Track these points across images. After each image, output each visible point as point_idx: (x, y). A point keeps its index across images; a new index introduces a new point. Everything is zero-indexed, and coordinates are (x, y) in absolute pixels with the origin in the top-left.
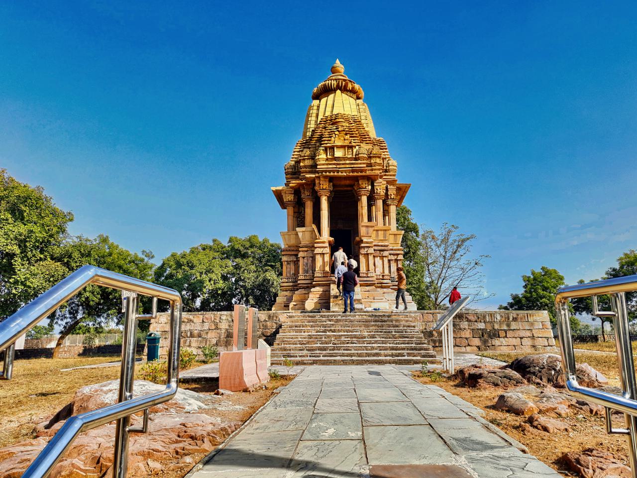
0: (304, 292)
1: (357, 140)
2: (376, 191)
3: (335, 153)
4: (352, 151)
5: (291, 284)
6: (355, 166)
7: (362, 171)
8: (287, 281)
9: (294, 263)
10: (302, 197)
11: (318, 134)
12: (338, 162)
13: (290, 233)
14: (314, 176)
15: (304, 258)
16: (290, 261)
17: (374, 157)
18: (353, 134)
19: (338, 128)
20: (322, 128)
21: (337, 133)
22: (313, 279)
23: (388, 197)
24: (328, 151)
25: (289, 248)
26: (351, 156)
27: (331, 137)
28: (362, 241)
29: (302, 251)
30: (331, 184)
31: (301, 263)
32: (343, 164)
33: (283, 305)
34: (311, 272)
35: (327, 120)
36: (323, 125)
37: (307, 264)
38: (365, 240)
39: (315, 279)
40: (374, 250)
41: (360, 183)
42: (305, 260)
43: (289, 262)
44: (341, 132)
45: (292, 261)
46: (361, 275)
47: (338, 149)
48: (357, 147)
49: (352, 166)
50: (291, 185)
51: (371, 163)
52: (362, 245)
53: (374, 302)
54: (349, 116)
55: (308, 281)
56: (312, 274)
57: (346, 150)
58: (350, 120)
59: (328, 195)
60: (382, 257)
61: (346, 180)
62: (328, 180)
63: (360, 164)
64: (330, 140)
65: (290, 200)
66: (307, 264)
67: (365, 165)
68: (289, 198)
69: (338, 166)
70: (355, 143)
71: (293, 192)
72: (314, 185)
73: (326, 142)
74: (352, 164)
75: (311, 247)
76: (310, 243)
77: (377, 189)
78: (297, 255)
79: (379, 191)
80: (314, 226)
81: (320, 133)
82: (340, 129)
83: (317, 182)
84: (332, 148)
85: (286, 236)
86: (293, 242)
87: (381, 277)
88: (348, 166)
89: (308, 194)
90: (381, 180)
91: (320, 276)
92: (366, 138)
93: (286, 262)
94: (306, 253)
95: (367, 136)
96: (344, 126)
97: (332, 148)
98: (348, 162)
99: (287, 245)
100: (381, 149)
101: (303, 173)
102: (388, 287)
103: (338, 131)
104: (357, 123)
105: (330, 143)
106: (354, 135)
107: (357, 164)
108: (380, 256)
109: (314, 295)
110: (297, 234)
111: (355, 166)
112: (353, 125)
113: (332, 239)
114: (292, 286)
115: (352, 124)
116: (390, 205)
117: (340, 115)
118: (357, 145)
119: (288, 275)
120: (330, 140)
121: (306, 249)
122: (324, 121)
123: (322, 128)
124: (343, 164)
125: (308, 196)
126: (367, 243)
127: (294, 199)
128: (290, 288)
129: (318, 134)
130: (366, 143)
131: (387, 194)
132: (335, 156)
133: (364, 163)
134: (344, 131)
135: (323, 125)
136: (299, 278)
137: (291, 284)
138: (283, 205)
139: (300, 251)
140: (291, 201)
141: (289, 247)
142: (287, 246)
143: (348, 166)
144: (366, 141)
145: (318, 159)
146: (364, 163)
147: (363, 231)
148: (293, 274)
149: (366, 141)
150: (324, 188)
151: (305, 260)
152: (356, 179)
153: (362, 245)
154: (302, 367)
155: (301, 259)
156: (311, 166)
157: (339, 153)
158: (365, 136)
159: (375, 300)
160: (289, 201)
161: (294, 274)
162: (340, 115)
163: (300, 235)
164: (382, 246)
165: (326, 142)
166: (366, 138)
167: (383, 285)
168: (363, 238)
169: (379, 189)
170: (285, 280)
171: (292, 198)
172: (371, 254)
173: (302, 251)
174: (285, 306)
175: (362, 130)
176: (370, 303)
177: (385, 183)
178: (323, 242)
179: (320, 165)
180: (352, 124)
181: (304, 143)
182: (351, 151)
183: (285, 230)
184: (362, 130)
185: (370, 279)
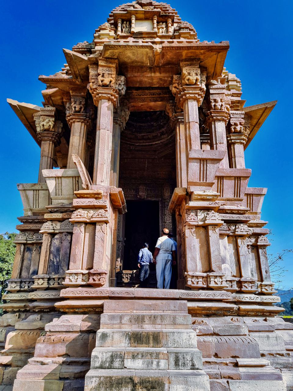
2: (213, 104)
3: (133, 25)
4: (167, 27)
8: (18, 288)
15: (53, 235)
16: (33, 244)
24: (120, 25)
25: (35, 217)
28: (189, 195)
29: (52, 220)
30: (123, 78)
38: (197, 191)
41: (185, 71)
43: (31, 247)
46: (189, 283)
47: (139, 22)
52: (192, 204)
61: (155, 72)
62: (114, 65)
66: (58, 250)
68: (44, 123)
71: (53, 114)
77: (215, 101)
79: (219, 105)
83: (92, 72)
87: (235, 287)
91: (80, 282)
93: (23, 247)
97: (127, 20)
99: (31, 210)
108: (228, 236)
109: (50, 347)
113: (117, 190)
121: (59, 216)
128: (22, 305)
132: (132, 30)
141: (34, 214)
150: (107, 81)
153: (192, 204)
159: (241, 370)
160: (45, 130)
164: (232, 212)
167: (243, 307)
168: (192, 189)
169: (218, 98)
170: (14, 285)
171: (51, 124)
172: (215, 225)
173: (52, 220)
178: (97, 196)
182: (164, 26)
185: (217, 295)
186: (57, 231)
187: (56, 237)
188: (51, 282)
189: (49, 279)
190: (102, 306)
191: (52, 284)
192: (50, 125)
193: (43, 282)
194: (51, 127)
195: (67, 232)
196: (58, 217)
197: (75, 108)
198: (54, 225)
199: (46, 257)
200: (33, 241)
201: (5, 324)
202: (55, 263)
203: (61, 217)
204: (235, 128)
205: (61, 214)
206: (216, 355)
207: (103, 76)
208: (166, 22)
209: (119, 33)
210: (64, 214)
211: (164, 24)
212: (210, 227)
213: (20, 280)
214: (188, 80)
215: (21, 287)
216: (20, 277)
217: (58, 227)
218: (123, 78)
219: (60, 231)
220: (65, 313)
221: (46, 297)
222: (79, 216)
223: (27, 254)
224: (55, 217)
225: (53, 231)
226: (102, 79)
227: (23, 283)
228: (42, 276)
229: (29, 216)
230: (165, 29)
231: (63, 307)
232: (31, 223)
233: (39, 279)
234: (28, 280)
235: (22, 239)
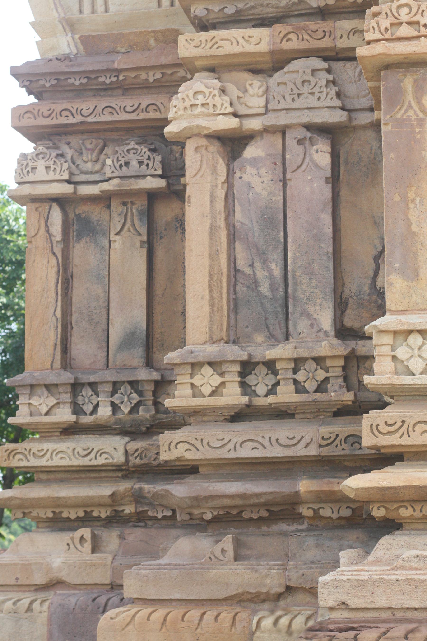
0: (239, 576)
5: (113, 449)
8: (65, 415)
15: (233, 144)
16: (105, 199)
25: (92, 64)
34: (326, 320)
37: (277, 220)
42: (256, 175)
43: (96, 213)
45: (125, 196)
55: (283, 431)
56: (330, 347)
66: (277, 220)
93: (56, 215)
94: (254, 93)
99: (70, 25)
114: (124, 471)
119: (85, 350)
121: (257, 41)
128: (104, 491)
136: (178, 399)
137: (113, 449)
139: (188, 69)
141: (90, 44)
142: (65, 44)
148: (128, 341)
155: (203, 175)
161: (151, 342)
186: (254, 124)
187: (251, 152)
188: (260, 382)
189: (247, 367)
191: (261, 390)
193: (216, 380)
195: (308, 127)
196: (250, 48)
198: (234, 91)
199: (213, 257)
200: (105, 186)
201: (39, 579)
202: (265, 288)
203: (264, 47)
205: (263, 33)
210: (280, 28)
213: (67, 377)
215: (77, 410)
216: (67, 363)
217: (256, 103)
219: (272, 120)
220: (391, 526)
221: (246, 452)
222: (405, 31)
223: (84, 254)
224: (237, 49)
225: (231, 123)
227: (87, 392)
228: (212, 351)
229: (66, 58)
231: (388, 495)
232: (79, 92)
233: (196, 366)
234: (110, 376)
235: (51, 176)
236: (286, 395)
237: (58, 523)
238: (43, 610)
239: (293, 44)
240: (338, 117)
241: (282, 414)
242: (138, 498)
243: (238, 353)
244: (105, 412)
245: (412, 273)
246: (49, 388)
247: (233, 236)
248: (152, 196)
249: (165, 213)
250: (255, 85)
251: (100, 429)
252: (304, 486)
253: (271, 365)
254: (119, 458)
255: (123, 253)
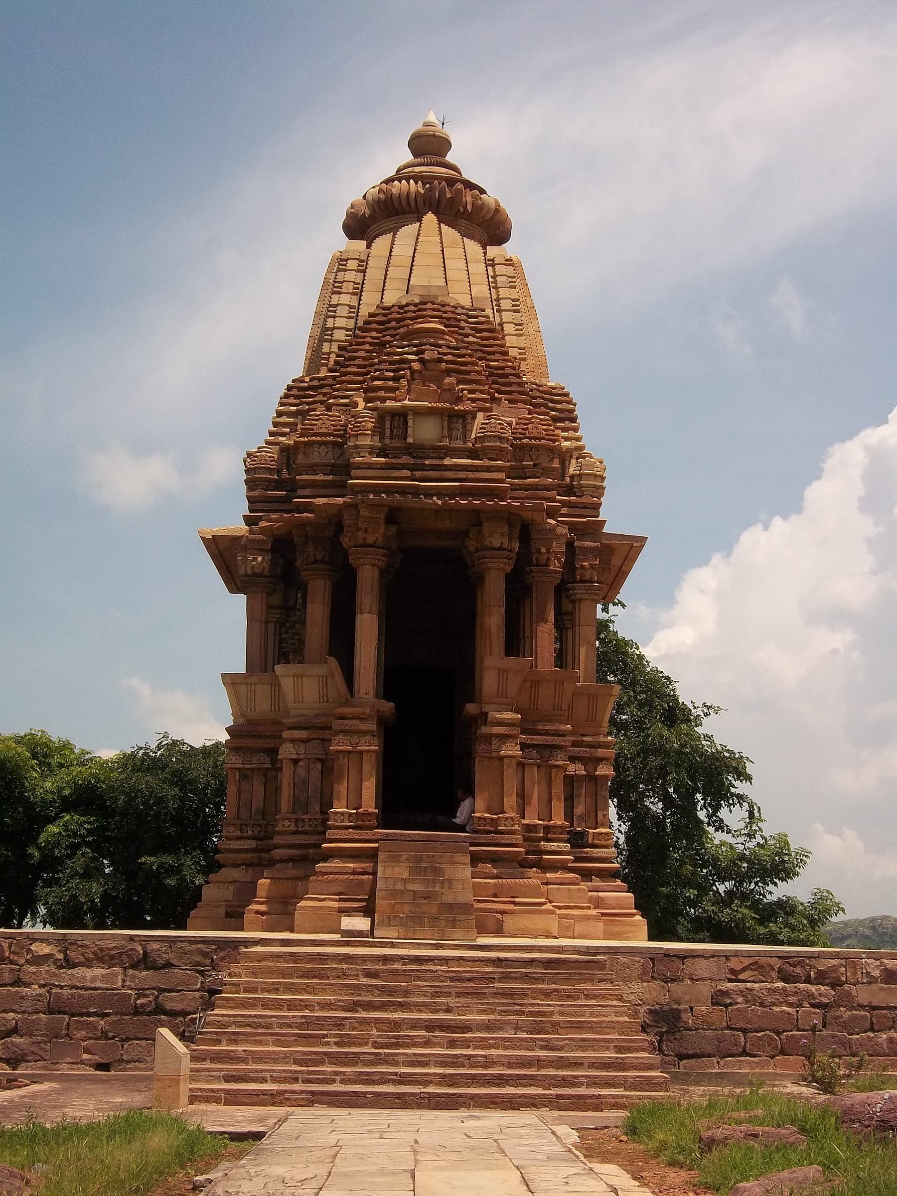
1: (482, 392)
2: (534, 558)
4: (464, 427)
5: (253, 844)
6: (471, 475)
7: (491, 493)
8: (238, 833)
9: (265, 775)
10: (298, 563)
11: (357, 362)
12: (419, 461)
13: (254, 679)
14: (340, 500)
15: (295, 762)
16: (253, 770)
17: (532, 447)
18: (468, 373)
19: (423, 352)
20: (371, 344)
21: (416, 366)
22: (324, 833)
23: (574, 576)
24: (388, 424)
26: (459, 444)
27: (396, 379)
29: (292, 741)
31: (286, 777)
32: (433, 468)
33: (222, 911)
34: (318, 810)
35: (389, 321)
36: (374, 334)
39: (330, 834)
40: (524, 746)
42: (301, 771)
44: (428, 365)
45: (258, 769)
48: (480, 415)
49: (462, 475)
50: (263, 524)
51: (524, 468)
52: (485, 730)
53: (513, 912)
54: (459, 311)
55: (306, 837)
56: (319, 816)
57: (446, 423)
58: (463, 324)
59: (380, 563)
60: (548, 770)
62: (383, 516)
63: (489, 469)
64: (394, 389)
65: (257, 571)
67: (502, 475)
69: (418, 474)
70: (473, 400)
72: (340, 528)
73: (382, 393)
74: (465, 468)
75: (321, 728)
76: (317, 716)
78: (273, 752)
80: (333, 663)
81: (364, 359)
82: (427, 356)
83: (347, 520)
84: (401, 415)
85: (243, 689)
86: (263, 705)
88: (449, 474)
89: (319, 557)
90: (553, 522)
92: (510, 384)
93: (237, 774)
95: (513, 379)
96: (440, 346)
98: (447, 461)
99: (243, 716)
100: (555, 420)
101: (303, 487)
102: (563, 867)
103: (422, 361)
104: (485, 334)
105: (395, 399)
106: (473, 376)
107: (477, 469)
110: (276, 683)
111: (471, 475)
112: (471, 339)
113: (388, 706)
114: (255, 851)
115: (467, 336)
116: (581, 600)
117: (429, 305)
118: (481, 410)
119: (244, 814)
120: (394, 389)
122: (379, 323)
123: (371, 344)
124: (433, 468)
125: (316, 562)
126: (501, 723)
127: (273, 564)
128: (250, 855)
129: (357, 362)
130: (510, 401)
131: (570, 565)
133: (499, 469)
134: (440, 361)
135: (374, 334)
137: (253, 844)
138: (234, 582)
139: (286, 740)
140: (260, 575)
141: (250, 722)
142: (241, 721)
143: (449, 474)
144: (510, 393)
145: (357, 447)
146: (499, 469)
147: (489, 682)
149: (510, 393)
150: (371, 540)
151: (301, 771)
152: (477, 518)
153: (485, 730)
154: (280, 1111)
156: (333, 465)
157: (425, 431)
158: (507, 376)
160: (255, 575)
162: (429, 305)
163: (287, 684)
164: (547, 733)
165: (382, 393)
166: (510, 384)
170: (232, 829)
173: (292, 741)
174: (228, 915)
175: (497, 356)
176: (499, 916)
177: (564, 530)
179: (359, 466)
180: (467, 336)
181: (310, 388)
183: (241, 668)
184: (497, 356)
185: (506, 839)
186: (302, 757)
189: (297, 820)
190: (376, 850)
192: (264, 569)
194: (266, 570)
197: (315, 555)
202: (302, 800)
204: (581, 575)
206: (495, 896)
207: (366, 531)
208: (465, 420)
209: (387, 441)
210: (310, 731)
211: (460, 421)
212: (506, 760)
214: (490, 542)
215: (242, 832)
216: (238, 818)
218: (394, 529)
219: (307, 756)
226: (365, 535)
230: (461, 431)
233: (284, 820)
236: (307, 828)
237: (236, 865)
238: (231, 888)
239: (313, 736)
240: (324, 757)
241: (305, 833)
242: (260, 858)
243: (294, 816)
244: (250, 833)
245: (339, 800)
246: (234, 825)
247: (294, 784)
248: (267, 769)
249: (270, 774)
250: (302, 746)
251: (248, 838)
252: (311, 851)
253: (303, 820)
254: (254, 846)
255: (258, 786)
